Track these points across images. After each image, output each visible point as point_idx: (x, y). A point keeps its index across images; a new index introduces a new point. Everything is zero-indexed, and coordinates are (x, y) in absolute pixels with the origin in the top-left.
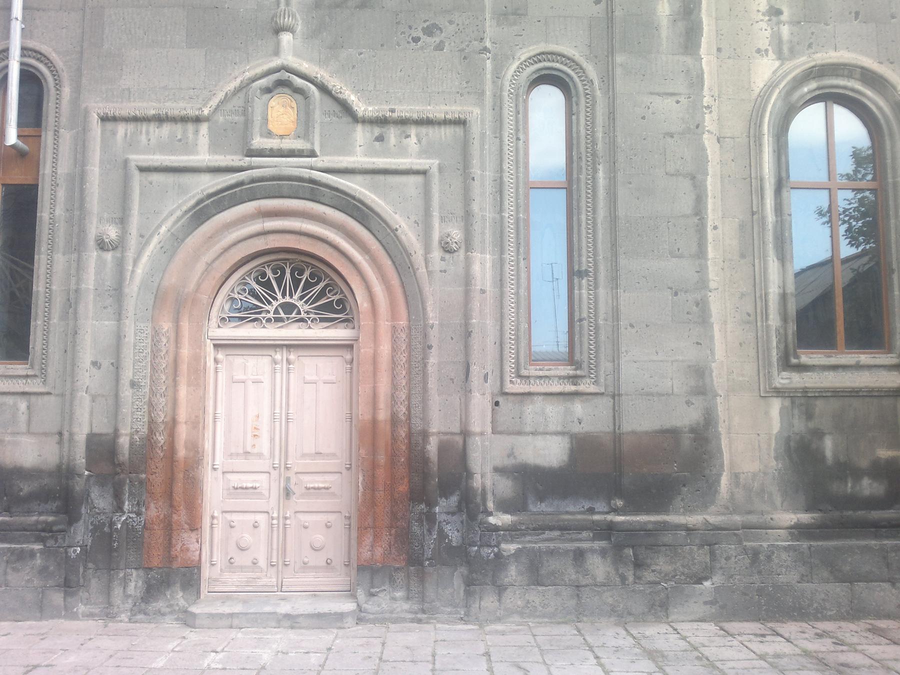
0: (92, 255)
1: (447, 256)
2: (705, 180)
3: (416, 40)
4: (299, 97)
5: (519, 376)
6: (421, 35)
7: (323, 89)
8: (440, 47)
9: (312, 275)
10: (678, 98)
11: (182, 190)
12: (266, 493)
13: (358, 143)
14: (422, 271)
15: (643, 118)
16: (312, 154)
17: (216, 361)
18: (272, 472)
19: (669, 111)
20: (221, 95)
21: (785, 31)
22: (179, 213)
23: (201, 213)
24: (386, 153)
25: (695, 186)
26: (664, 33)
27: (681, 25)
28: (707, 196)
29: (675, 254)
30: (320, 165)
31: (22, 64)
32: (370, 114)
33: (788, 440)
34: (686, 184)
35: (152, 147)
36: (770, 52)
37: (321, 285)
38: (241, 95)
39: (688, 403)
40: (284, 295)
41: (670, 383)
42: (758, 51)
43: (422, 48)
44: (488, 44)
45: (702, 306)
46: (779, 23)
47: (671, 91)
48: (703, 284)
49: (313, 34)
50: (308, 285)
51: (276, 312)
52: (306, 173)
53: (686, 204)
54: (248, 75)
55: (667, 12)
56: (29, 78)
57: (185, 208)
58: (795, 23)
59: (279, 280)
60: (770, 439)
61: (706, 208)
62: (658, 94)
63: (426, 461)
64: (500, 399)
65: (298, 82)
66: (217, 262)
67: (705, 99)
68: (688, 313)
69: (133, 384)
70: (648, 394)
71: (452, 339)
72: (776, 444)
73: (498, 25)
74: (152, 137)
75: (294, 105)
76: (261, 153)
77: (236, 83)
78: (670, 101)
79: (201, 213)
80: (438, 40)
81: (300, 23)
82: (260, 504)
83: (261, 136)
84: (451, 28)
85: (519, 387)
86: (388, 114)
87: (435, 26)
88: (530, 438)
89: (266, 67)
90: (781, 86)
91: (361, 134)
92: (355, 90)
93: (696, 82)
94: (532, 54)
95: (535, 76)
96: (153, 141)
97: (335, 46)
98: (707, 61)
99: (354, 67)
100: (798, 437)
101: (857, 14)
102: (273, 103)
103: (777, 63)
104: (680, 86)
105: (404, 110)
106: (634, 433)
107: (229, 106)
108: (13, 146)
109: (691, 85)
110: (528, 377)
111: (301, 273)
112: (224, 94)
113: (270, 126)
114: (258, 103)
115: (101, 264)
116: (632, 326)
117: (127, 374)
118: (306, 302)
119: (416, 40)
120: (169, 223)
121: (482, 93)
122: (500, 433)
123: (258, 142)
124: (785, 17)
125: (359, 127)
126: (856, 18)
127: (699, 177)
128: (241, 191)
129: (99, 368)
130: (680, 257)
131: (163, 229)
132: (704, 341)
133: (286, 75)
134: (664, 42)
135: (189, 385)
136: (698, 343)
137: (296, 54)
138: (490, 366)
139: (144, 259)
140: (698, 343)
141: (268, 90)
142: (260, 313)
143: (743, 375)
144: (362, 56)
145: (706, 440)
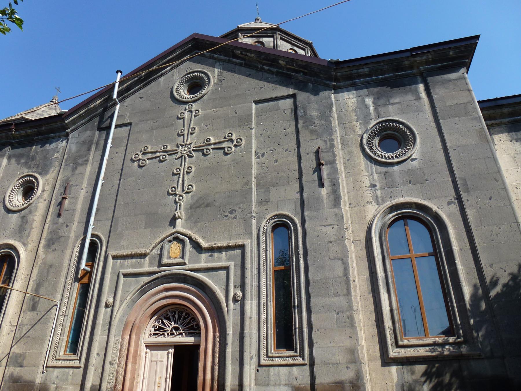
0: (102, 310)
2: (348, 260)
3: (226, 216)
5: (268, 357)
6: (228, 214)
7: (190, 238)
8: (235, 218)
9: (186, 314)
10: (332, 226)
11: (138, 282)
14: (225, 309)
15: (318, 236)
16: (185, 264)
17: (146, 353)
19: (329, 232)
20: (153, 245)
21: (379, 193)
22: (134, 291)
23: (143, 291)
24: (213, 261)
25: (343, 263)
26: (325, 201)
27: (332, 197)
28: (349, 267)
29: (336, 295)
30: (187, 268)
31: (91, 240)
33: (403, 386)
34: (339, 262)
35: (129, 266)
36: (373, 202)
37: (189, 318)
38: (161, 244)
39: (348, 368)
40: (175, 323)
41: (338, 358)
42: (368, 202)
43: (228, 219)
44: (254, 214)
45: (351, 318)
46: (376, 190)
47: (329, 224)
48: (350, 308)
49: (188, 219)
50: (185, 318)
51: (171, 330)
53: (340, 271)
54: (164, 236)
55: (326, 193)
56: (93, 244)
57: (137, 289)
58: (383, 188)
59: (173, 316)
60: (393, 386)
61: (349, 273)
62: (324, 226)
64: (259, 369)
65: (181, 237)
66: (148, 310)
67: (345, 226)
68: (344, 322)
69: (111, 363)
70: (327, 364)
72: (396, 388)
73: (259, 206)
74: (129, 262)
75: (180, 246)
76: (166, 265)
77: (159, 240)
78: (329, 228)
79: (143, 291)
80: (234, 215)
81: (184, 215)
84: (240, 210)
85: (269, 362)
86: (214, 246)
87: (233, 210)
88: (273, 387)
89: (170, 233)
90: (378, 215)
91: (204, 256)
92: (202, 238)
93: (340, 218)
94: (271, 216)
95: (274, 224)
96: (129, 264)
97: (196, 222)
98: (346, 209)
100: (408, 384)
101: (410, 182)
102: (172, 246)
103: (377, 206)
104: (334, 221)
105: (220, 243)
106: (322, 384)
108: (83, 269)
109: (338, 220)
110: (272, 357)
111: (182, 313)
114: (167, 246)
115: (106, 313)
116: (318, 330)
117: (109, 358)
118: (171, 324)
119: (226, 216)
120: (131, 295)
121: (251, 234)
122: (259, 385)
123: (165, 261)
124: (378, 186)
126: (410, 183)
127: (345, 259)
130: (339, 296)
131: (128, 298)
132: (353, 336)
134: (325, 204)
135: (132, 363)
136: (350, 337)
137: (182, 227)
138: (255, 352)
139: (120, 310)
140: (350, 337)
141: (170, 241)
142: (165, 331)
143: (375, 352)
145: (358, 387)
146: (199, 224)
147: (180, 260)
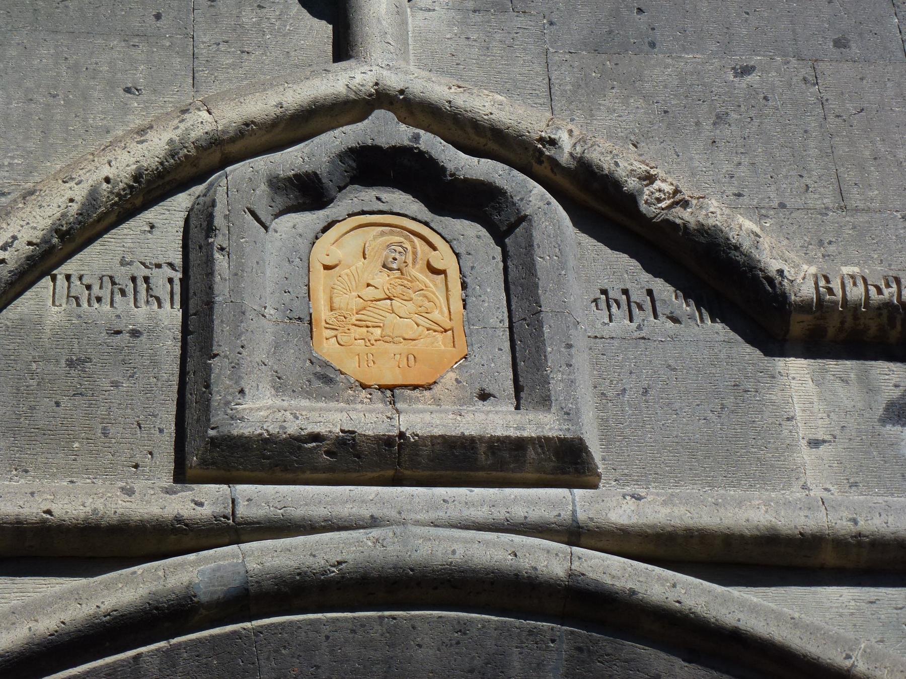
4: (470, 231)
13: (803, 432)
16: (568, 463)
32: (856, 293)
52: (550, 560)
54: (202, 124)
75: (444, 258)
76: (284, 458)
83: (280, 385)
99: (720, 119)
102: (327, 248)
107: (91, 261)
112: (80, 193)
113: (327, 347)
123: (261, 409)
125: (796, 371)
128: (167, 654)
133: (387, 130)
144: (753, 79)
146: (662, 72)
147: (499, 421)
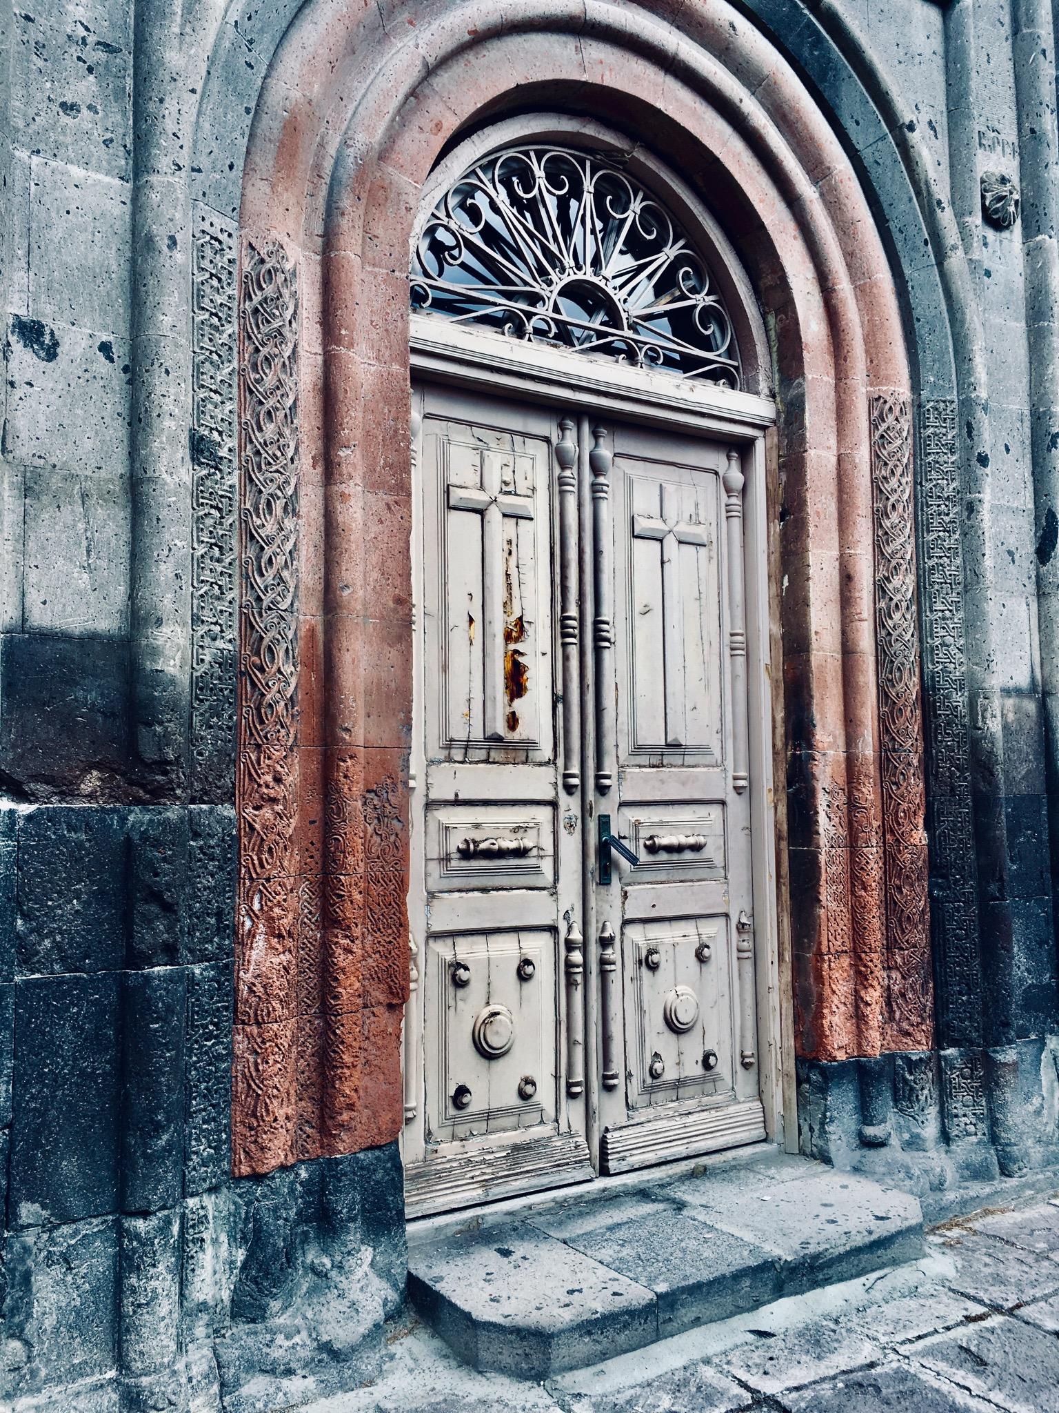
1: (990, 234)
12: (718, 860)
18: (564, 799)
63: (980, 761)
71: (1008, 450)
82: (540, 909)
129: (51, 354)
